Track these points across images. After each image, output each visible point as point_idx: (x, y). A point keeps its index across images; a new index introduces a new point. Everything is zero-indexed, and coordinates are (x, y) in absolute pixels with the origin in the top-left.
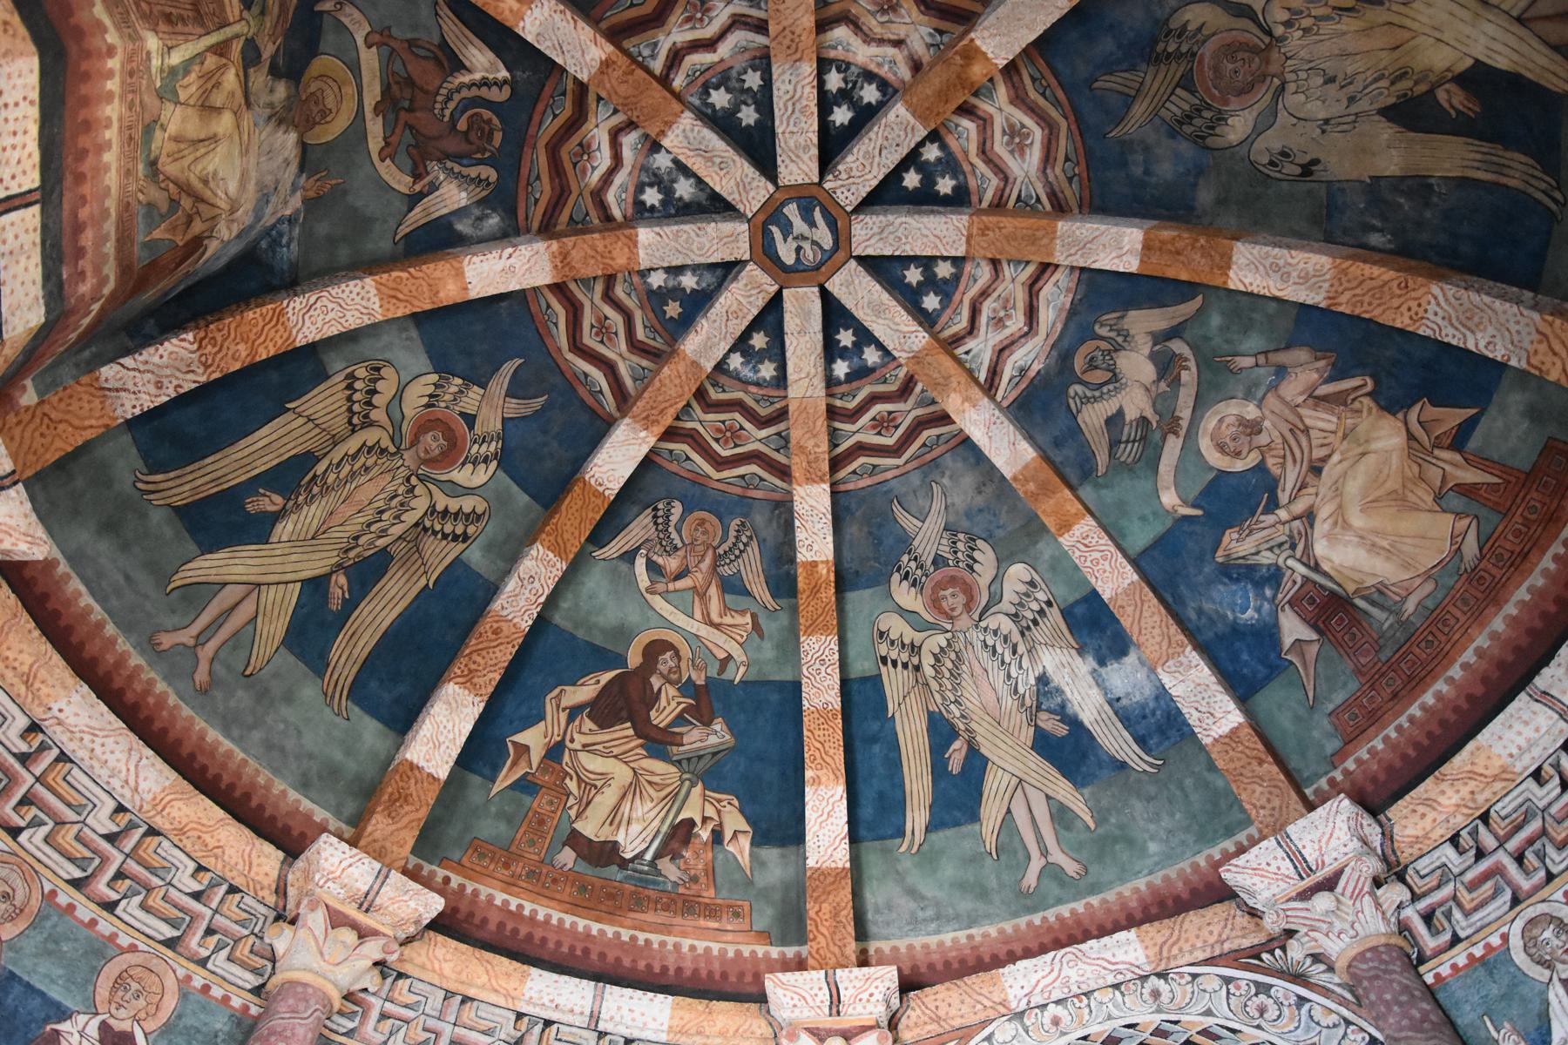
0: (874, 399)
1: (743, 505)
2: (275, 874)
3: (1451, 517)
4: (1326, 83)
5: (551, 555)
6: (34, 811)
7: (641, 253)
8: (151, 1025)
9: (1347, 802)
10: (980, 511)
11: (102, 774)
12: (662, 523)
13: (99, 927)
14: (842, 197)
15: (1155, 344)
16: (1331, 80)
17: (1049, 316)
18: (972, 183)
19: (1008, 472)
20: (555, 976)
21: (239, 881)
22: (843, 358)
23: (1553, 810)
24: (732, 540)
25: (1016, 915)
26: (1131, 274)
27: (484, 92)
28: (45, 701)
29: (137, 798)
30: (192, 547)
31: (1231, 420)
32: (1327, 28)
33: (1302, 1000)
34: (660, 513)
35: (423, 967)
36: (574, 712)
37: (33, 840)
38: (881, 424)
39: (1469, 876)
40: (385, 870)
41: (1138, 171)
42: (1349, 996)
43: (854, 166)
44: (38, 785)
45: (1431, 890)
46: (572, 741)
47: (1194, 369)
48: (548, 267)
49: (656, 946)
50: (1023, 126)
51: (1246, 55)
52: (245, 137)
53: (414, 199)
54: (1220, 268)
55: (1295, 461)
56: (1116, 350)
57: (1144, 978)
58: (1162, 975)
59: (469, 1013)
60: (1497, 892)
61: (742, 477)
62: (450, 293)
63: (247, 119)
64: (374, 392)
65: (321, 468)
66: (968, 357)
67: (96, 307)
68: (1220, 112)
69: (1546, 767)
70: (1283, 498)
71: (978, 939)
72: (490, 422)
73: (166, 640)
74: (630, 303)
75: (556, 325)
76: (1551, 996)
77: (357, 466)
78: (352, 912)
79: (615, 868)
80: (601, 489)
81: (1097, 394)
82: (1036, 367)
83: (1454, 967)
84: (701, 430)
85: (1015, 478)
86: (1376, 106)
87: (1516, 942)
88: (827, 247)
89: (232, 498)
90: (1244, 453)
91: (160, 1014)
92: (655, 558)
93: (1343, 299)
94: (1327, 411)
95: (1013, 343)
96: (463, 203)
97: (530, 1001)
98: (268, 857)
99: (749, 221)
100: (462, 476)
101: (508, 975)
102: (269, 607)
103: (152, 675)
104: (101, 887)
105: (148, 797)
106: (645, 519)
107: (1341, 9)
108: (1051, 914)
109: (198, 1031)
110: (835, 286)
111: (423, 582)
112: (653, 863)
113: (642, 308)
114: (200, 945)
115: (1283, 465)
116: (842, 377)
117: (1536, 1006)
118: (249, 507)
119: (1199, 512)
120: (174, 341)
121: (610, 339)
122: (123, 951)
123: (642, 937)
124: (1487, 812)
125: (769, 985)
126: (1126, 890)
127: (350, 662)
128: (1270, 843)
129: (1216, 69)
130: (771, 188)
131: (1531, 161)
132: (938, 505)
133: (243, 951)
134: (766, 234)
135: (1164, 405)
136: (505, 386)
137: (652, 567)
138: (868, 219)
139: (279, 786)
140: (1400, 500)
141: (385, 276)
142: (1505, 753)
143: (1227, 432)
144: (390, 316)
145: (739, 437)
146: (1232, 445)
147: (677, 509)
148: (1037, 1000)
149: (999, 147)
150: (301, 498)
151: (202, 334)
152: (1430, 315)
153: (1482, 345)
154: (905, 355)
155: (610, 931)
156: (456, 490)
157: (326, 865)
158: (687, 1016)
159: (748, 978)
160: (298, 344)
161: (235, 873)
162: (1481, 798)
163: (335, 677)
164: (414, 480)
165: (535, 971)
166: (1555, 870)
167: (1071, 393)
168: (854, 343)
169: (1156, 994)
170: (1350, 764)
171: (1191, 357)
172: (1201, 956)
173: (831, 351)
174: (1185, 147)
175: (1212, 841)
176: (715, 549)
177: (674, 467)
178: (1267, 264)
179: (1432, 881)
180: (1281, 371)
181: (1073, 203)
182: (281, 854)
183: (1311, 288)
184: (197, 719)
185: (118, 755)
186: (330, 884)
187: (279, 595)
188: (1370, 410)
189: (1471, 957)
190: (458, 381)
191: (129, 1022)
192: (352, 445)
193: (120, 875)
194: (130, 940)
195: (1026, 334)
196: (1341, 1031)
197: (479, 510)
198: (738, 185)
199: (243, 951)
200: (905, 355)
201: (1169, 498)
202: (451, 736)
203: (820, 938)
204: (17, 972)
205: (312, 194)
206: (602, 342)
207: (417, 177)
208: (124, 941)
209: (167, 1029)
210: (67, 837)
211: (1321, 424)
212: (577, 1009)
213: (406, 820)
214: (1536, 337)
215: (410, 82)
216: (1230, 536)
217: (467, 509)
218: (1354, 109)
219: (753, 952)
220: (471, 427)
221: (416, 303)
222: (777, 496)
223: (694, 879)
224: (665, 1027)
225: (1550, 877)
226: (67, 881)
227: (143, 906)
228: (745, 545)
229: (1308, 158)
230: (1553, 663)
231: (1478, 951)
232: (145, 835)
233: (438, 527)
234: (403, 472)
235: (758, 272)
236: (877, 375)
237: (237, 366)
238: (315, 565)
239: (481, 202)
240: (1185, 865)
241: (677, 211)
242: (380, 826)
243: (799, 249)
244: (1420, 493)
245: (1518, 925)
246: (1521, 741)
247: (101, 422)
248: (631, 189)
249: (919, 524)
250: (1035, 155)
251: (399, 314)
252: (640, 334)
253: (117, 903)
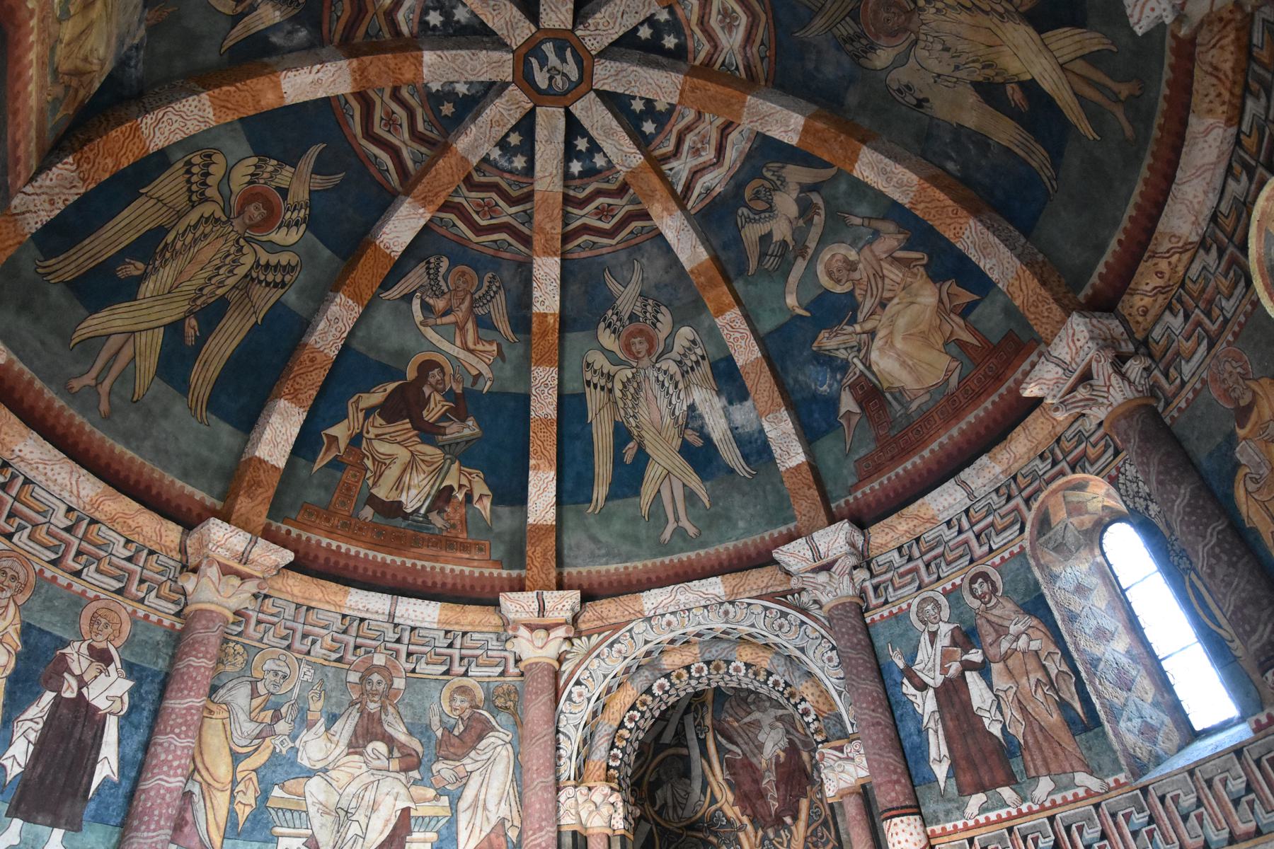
0: (599, 193)
1: (495, 263)
2: (178, 541)
3: (948, 358)
4: (943, 50)
5: (351, 302)
6: (18, 520)
7: (425, 70)
8: (118, 643)
9: (847, 525)
10: (666, 285)
11: (55, 489)
12: (432, 274)
13: (74, 588)
14: (589, 43)
15: (801, 192)
16: (947, 49)
17: (731, 154)
18: (690, 44)
19: (688, 268)
20: (366, 593)
21: (155, 547)
22: (579, 160)
23: (951, 544)
24: (485, 288)
25: (655, 556)
26: (792, 146)
28: (9, 446)
29: (80, 502)
30: (82, 311)
31: (838, 257)
32: (952, 14)
33: (803, 623)
34: (432, 266)
35: (280, 590)
36: (369, 412)
37: (21, 539)
38: (602, 213)
39: (902, 570)
40: (254, 538)
41: (810, 66)
42: (827, 624)
43: (601, 22)
44: (16, 503)
45: (882, 574)
46: (368, 432)
47: (823, 217)
48: (349, 79)
49: (428, 569)
50: (734, 11)
51: (897, 11)
52: (110, 10)
53: (236, 19)
54: (850, 159)
55: (872, 295)
56: (774, 190)
57: (721, 604)
58: (732, 603)
59: (312, 617)
60: (913, 581)
61: (495, 241)
62: (269, 101)
64: (207, 174)
65: (170, 238)
66: (671, 173)
68: (872, 43)
69: (954, 520)
70: (860, 317)
71: (631, 569)
72: (300, 193)
73: (76, 385)
74: (413, 102)
75: (352, 116)
76: (922, 639)
77: (197, 235)
78: (235, 565)
79: (400, 519)
80: (388, 251)
81: (757, 217)
82: (718, 189)
83: (882, 616)
84: (465, 204)
85: (692, 272)
86: (970, 78)
87: (914, 608)
88: (573, 79)
89: (105, 269)
90: (844, 280)
91: (122, 635)
92: (427, 299)
93: (922, 206)
94: (898, 269)
95: (704, 169)
96: (277, 20)
97: (350, 608)
98: (172, 530)
99: (513, 52)
100: (279, 236)
101: (336, 593)
102: (143, 348)
103: (72, 411)
104: (69, 562)
105: (87, 500)
106: (420, 269)
107: (963, 6)
108: (675, 558)
109: (147, 642)
110: (577, 109)
111: (253, 320)
112: (425, 516)
113: (422, 107)
114: (137, 590)
115: (865, 296)
116: (576, 173)
117: (914, 642)
118: (120, 274)
119: (808, 314)
120: (60, 165)
121: (396, 129)
122: (92, 600)
123: (419, 564)
124: (919, 537)
125: (502, 599)
126: (721, 548)
127: (205, 383)
128: (802, 541)
129: (876, 13)
130: (534, 29)
131: (1045, 154)
132: (636, 277)
133: (165, 590)
134: (527, 64)
135: (800, 235)
136: (311, 166)
137: (426, 307)
138: (607, 63)
139: (169, 478)
140: (925, 337)
141: (217, 91)
142: (936, 508)
143: (836, 265)
144: (222, 121)
145: (494, 211)
146: (837, 274)
147: (445, 263)
148: (660, 611)
149: (714, 21)
150: (157, 263)
151: (79, 156)
152: (965, 237)
153: (988, 266)
154: (625, 169)
155: (398, 560)
156: (274, 248)
157: (215, 537)
158: (450, 614)
159: (487, 589)
160: (151, 152)
161: (152, 543)
162: (918, 530)
163: (196, 395)
164: (242, 242)
165: (353, 590)
166: (942, 575)
167: (740, 212)
168: (587, 148)
169: (726, 613)
170: (859, 494)
171: (822, 207)
172: (754, 594)
173: (570, 152)
174: (845, 60)
175: (776, 526)
176: (472, 294)
177: (442, 231)
178: (881, 166)
179: (883, 569)
180: (876, 234)
181: (762, 77)
182: (180, 528)
183: (903, 192)
184: (107, 439)
185: (63, 475)
186: (219, 549)
187: (150, 338)
188: (922, 276)
189: (891, 612)
190: (275, 162)
191: (105, 643)
192: (193, 217)
193: (79, 553)
194: (95, 593)
195: (714, 165)
196: (819, 641)
197: (293, 263)
198: (507, 24)
199: (165, 590)
200: (625, 169)
201: (791, 300)
202: (285, 437)
203: (534, 569)
204: (32, 622)
205: (153, 22)
206: (389, 131)
208: (91, 594)
209: (129, 643)
210: (41, 534)
211: (892, 276)
212: (380, 611)
213: (260, 499)
214: (1014, 275)
216: (824, 334)
217: (284, 263)
218: (958, 74)
219: (491, 573)
220: (285, 197)
221: (242, 110)
222: (520, 258)
223: (453, 526)
224: (436, 620)
225: (939, 578)
226: (48, 562)
227: (98, 571)
228: (495, 293)
229: (921, 96)
230: (971, 467)
231: (895, 610)
232: (89, 524)
233: (262, 277)
234: (233, 236)
235: (518, 92)
236: (602, 176)
237: (107, 176)
238: (172, 313)
239: (290, 20)
240: (757, 537)
241: (455, 31)
242: (244, 504)
243: (551, 79)
244: (937, 338)
245: (918, 600)
246: (946, 504)
247: (15, 241)
248: (418, 11)
249: (622, 289)
250: (739, 35)
251: (229, 120)
252: (420, 126)
253: (81, 571)
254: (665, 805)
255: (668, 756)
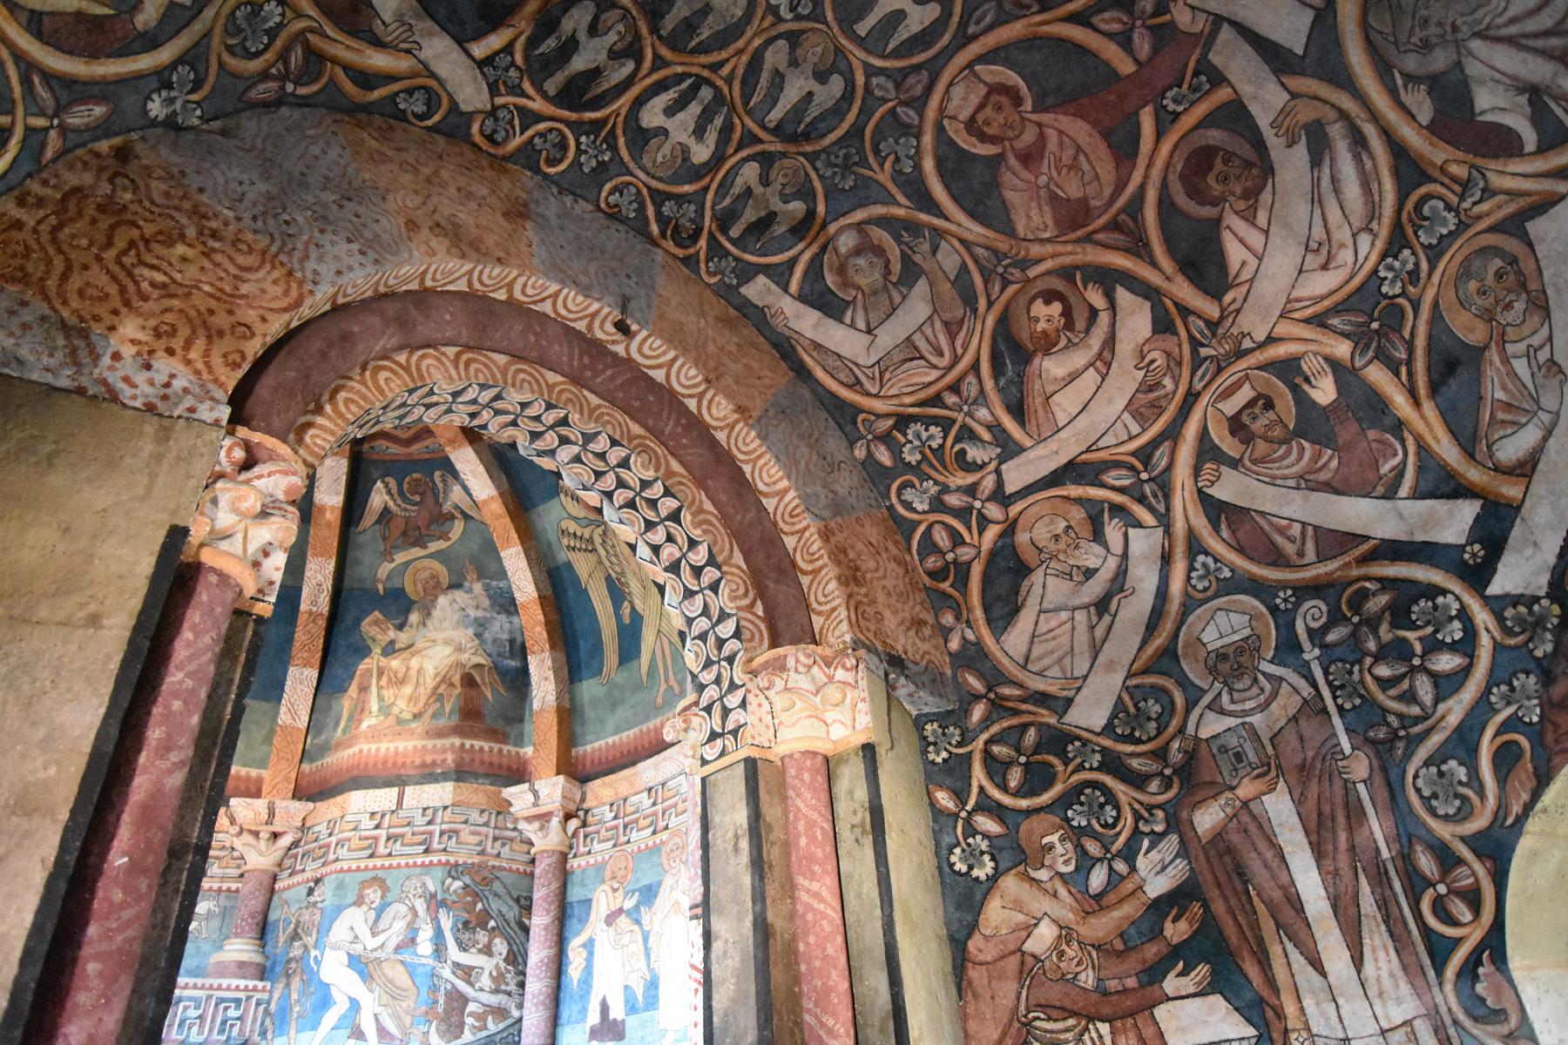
27: (394, 491)
53: (466, 517)
62: (497, 507)
63: (419, 645)
65: (614, 575)
67: (468, 743)
73: (659, 700)
192: (602, 552)
207: (453, 517)
215: (405, 534)
254: (1535, 94)
255: (1365, 26)
